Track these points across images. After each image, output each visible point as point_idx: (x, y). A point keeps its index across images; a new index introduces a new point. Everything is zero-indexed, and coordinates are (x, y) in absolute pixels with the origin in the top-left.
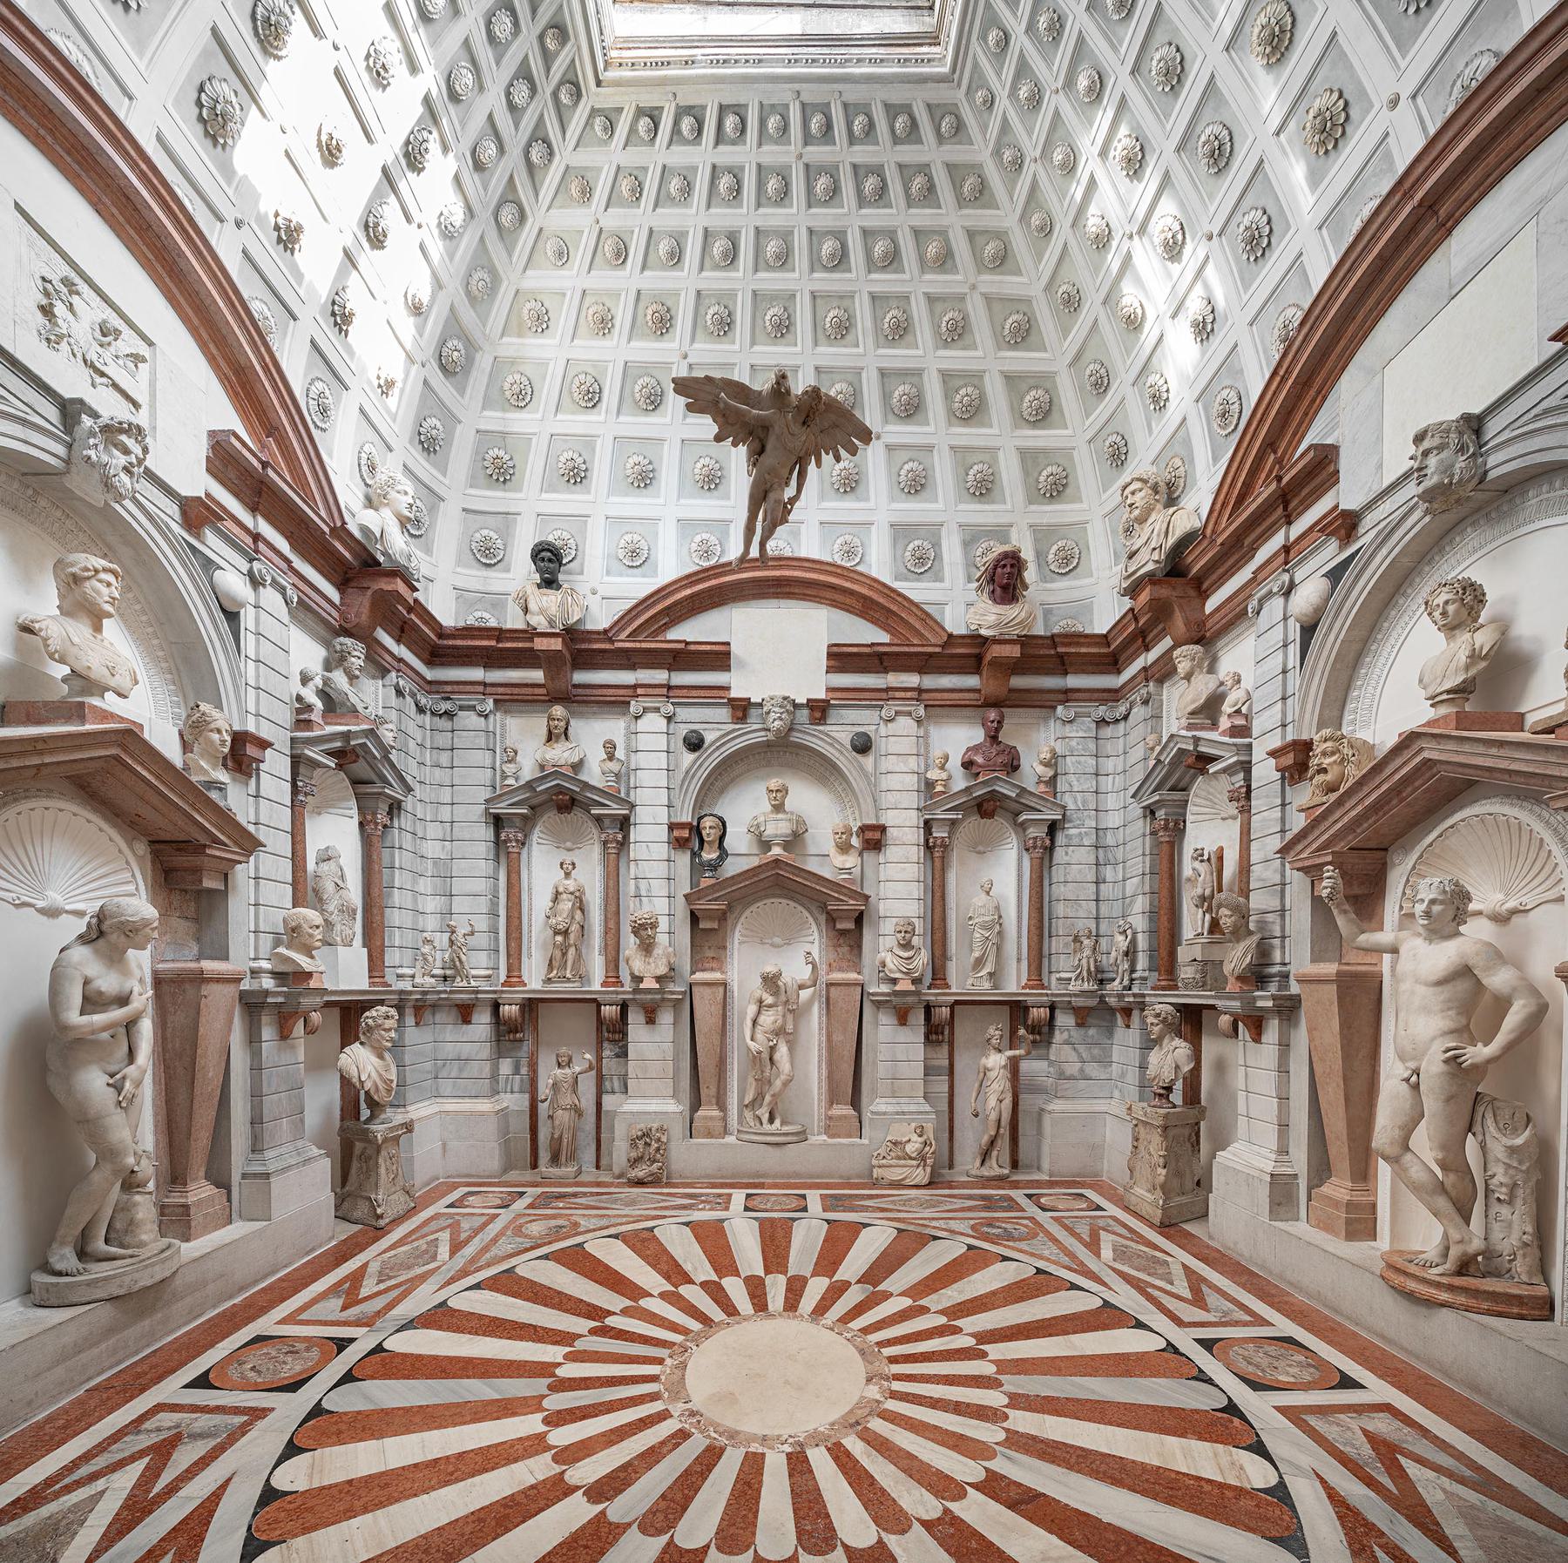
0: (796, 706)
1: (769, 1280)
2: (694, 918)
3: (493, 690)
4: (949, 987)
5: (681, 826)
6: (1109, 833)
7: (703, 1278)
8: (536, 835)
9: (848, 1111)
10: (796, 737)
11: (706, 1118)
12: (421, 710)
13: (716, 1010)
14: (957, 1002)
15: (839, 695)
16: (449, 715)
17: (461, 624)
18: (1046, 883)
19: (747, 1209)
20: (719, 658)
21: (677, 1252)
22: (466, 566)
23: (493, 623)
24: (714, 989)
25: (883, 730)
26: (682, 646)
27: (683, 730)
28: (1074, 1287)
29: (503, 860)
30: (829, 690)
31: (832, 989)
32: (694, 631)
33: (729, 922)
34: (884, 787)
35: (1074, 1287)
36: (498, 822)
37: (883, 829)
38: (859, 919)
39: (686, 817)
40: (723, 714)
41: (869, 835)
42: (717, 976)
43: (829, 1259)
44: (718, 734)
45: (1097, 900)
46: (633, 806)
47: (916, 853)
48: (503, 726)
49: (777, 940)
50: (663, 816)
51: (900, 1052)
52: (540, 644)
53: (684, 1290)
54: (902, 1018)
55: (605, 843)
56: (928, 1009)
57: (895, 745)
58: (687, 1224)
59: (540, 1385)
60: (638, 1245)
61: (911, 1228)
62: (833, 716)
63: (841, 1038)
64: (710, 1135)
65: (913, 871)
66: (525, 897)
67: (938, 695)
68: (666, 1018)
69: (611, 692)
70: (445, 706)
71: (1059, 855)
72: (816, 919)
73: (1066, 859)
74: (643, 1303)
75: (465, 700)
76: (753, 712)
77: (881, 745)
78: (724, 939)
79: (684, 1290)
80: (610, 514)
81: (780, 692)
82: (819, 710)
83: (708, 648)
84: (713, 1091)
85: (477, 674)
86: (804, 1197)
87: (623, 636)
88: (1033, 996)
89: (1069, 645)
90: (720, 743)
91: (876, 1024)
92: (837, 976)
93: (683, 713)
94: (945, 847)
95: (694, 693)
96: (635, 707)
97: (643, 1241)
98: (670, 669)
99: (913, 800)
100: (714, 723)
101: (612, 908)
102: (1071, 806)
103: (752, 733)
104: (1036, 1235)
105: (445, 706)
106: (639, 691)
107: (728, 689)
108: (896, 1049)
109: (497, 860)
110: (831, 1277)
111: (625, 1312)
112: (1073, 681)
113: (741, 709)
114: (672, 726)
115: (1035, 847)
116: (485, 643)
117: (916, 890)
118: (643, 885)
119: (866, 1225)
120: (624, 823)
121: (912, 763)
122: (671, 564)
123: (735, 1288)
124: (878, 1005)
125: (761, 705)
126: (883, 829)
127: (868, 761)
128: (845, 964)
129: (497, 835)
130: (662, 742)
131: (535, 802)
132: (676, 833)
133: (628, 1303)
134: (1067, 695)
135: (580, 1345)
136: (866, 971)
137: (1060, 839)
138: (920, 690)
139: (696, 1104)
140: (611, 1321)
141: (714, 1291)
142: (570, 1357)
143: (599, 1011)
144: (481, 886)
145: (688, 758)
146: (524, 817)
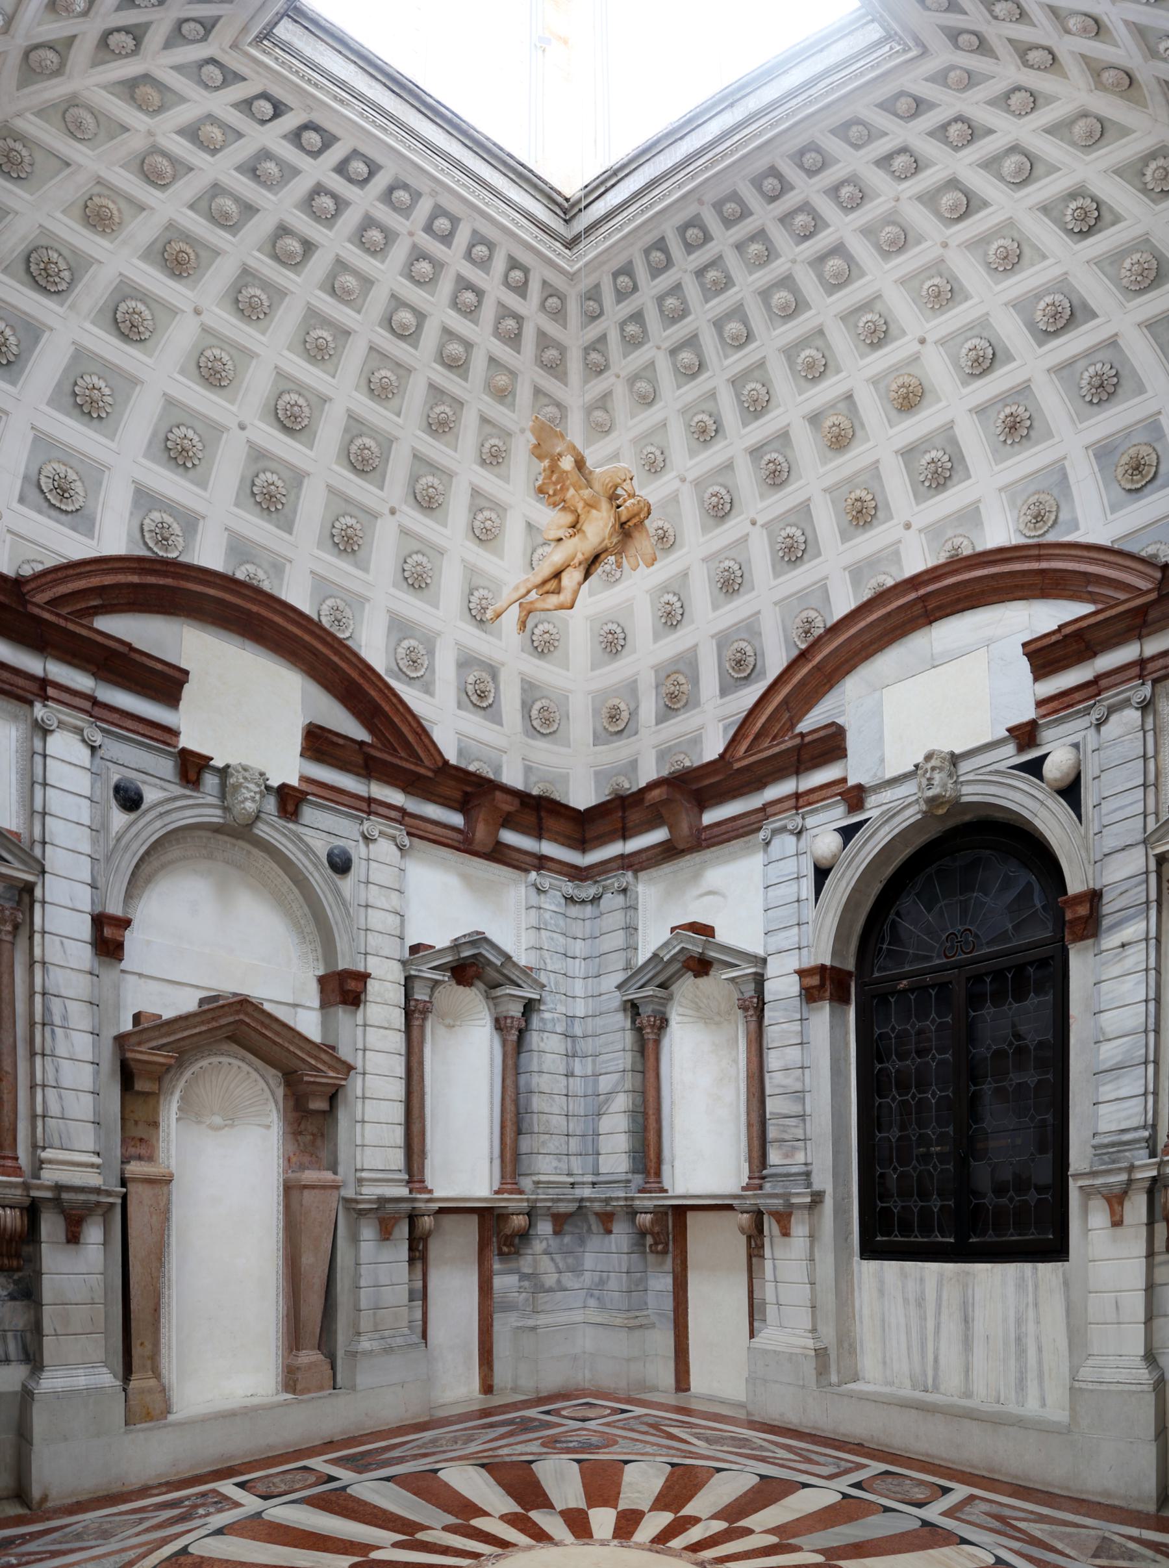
10: (262, 830)
20: (166, 683)
30: (304, 779)
37: (364, 977)
38: (333, 1098)
40: (166, 767)
47: (398, 1018)
49: (217, 1120)
56: (413, 1218)
62: (309, 814)
76: (210, 781)
77: (358, 869)
78: (156, 1111)
81: (256, 762)
82: (290, 801)
83: (159, 667)
93: (116, 749)
103: (203, 807)
107: (175, 733)
113: (192, 768)
114: (97, 760)
124: (361, 1213)
125: (224, 772)
126: (364, 977)
127: (347, 885)
128: (306, 1159)
130: (82, 783)
136: (341, 1169)
138: (402, 811)
145: (119, 818)
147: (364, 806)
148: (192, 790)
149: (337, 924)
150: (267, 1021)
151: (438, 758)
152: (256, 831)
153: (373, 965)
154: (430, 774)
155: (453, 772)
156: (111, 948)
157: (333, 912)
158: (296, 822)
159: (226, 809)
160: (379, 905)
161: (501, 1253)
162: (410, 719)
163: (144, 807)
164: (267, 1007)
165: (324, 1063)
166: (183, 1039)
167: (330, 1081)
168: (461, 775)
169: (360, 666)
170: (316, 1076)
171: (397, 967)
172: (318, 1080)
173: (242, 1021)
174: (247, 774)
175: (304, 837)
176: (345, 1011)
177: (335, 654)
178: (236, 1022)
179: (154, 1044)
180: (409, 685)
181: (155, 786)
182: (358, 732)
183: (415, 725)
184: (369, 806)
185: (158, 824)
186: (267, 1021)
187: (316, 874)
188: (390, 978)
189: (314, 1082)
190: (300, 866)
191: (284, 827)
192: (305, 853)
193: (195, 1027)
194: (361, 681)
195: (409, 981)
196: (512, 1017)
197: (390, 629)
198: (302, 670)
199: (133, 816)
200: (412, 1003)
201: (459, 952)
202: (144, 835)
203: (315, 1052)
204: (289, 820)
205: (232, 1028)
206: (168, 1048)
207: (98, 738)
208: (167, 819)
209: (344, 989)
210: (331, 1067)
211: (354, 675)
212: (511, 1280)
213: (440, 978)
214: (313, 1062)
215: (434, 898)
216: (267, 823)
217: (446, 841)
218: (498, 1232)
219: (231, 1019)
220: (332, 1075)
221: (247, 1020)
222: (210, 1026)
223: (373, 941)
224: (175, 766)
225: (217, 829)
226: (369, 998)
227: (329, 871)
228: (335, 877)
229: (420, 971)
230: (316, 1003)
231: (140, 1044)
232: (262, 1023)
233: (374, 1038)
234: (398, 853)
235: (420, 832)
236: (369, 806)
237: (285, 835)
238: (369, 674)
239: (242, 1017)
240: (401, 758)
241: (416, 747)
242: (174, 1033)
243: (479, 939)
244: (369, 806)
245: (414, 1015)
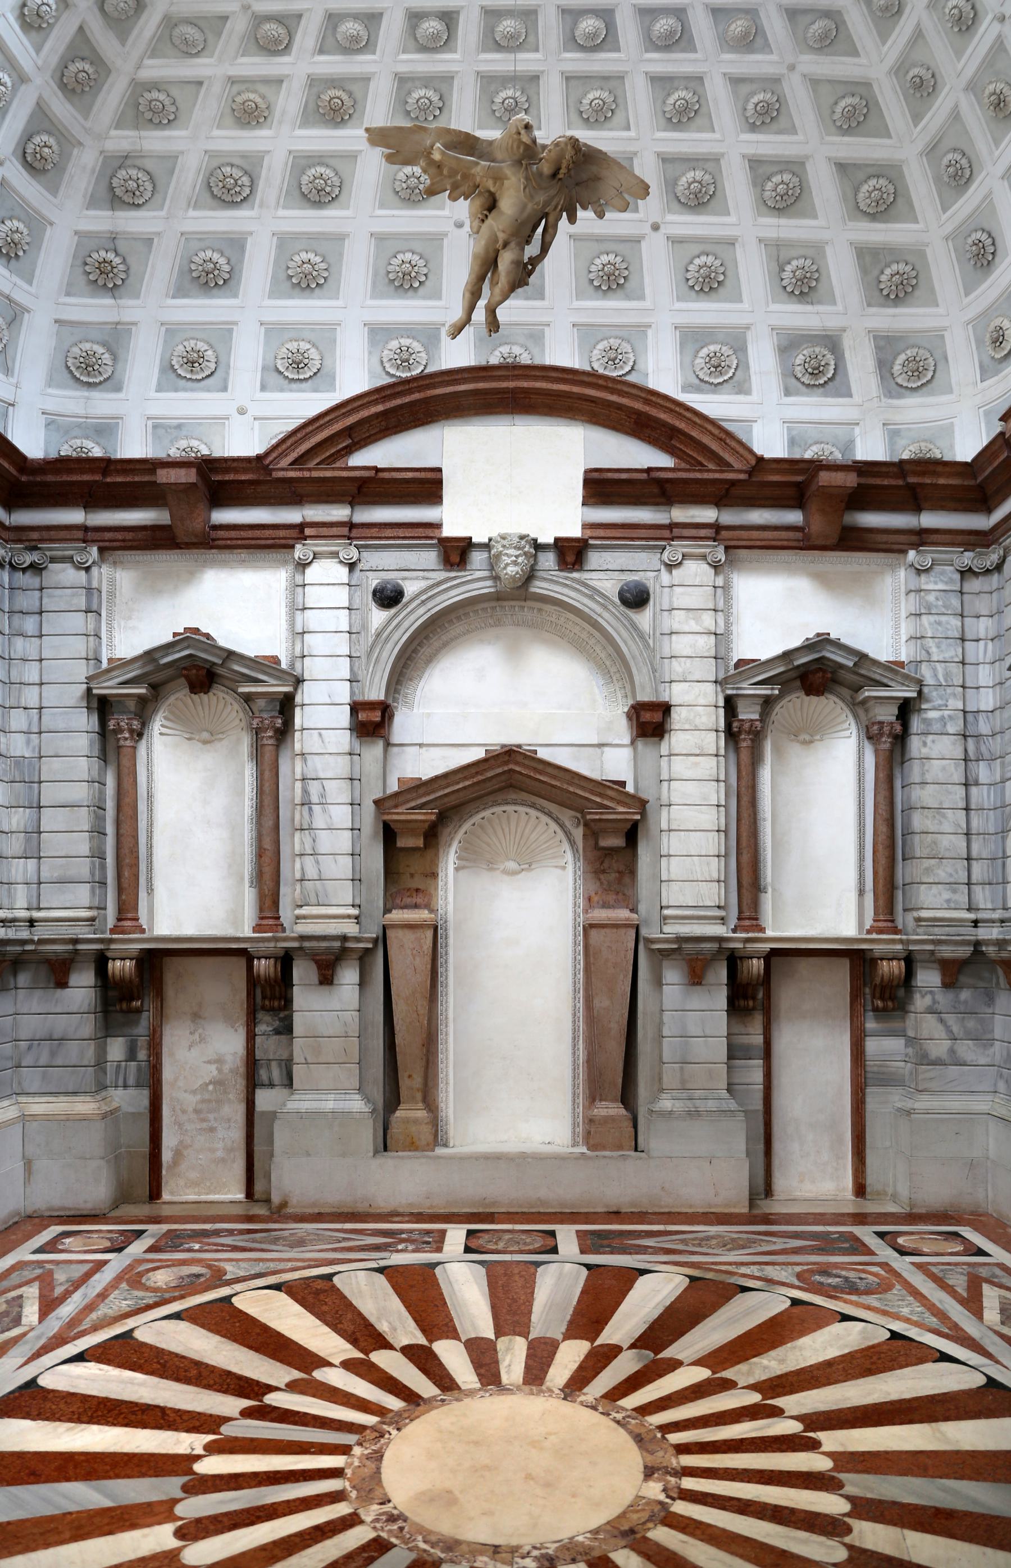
0: (538, 547)
1: (502, 1344)
2: (389, 834)
3: (97, 536)
4: (762, 930)
5: (371, 706)
6: (981, 717)
7: (405, 1341)
8: (157, 725)
9: (614, 1109)
11: (407, 1121)
13: (423, 963)
14: (774, 952)
15: (601, 533)
16: (35, 568)
17: (53, 455)
18: (898, 784)
21: (367, 1307)
22: (59, 386)
23: (97, 452)
24: (419, 933)
25: (665, 577)
28: (945, 1357)
29: (111, 756)
30: (586, 526)
31: (593, 933)
33: (443, 838)
34: (666, 653)
35: (945, 1357)
36: (102, 706)
39: (376, 693)
40: (430, 558)
41: (647, 716)
42: (423, 915)
43: (592, 1313)
44: (423, 584)
45: (967, 809)
46: (299, 681)
47: (713, 741)
48: (112, 582)
50: (343, 693)
51: (693, 1023)
52: (164, 476)
53: (380, 1358)
54: (696, 977)
55: (258, 732)
57: (683, 598)
58: (381, 1270)
59: (171, 1486)
60: (310, 1299)
61: (710, 1275)
62: (594, 559)
63: (606, 1003)
64: (412, 1146)
65: (709, 766)
66: (142, 807)
67: (744, 534)
68: (349, 976)
69: (267, 533)
70: (28, 558)
71: (915, 744)
72: (568, 834)
73: (925, 751)
74: (319, 1374)
75: (58, 549)
76: (478, 558)
77: (659, 599)
79: (380, 1358)
80: (265, 319)
84: (418, 1081)
85: (75, 516)
87: (284, 463)
88: (884, 944)
89: (923, 474)
90: (424, 596)
91: (658, 982)
92: (601, 915)
94: (757, 736)
95: (389, 532)
97: (317, 1293)
99: (708, 670)
100: (416, 571)
101: (269, 823)
102: (929, 680)
103: (474, 581)
104: (889, 1288)
105: (28, 558)
106: (308, 531)
107: (438, 526)
108: (690, 1019)
109: (104, 757)
110: (592, 1340)
111: (293, 1387)
112: (929, 520)
115: (881, 734)
116: (86, 478)
117: (714, 793)
118: (314, 788)
120: (286, 705)
121: (708, 620)
123: (451, 1354)
126: (666, 709)
127: (644, 618)
129: (103, 722)
131: (156, 678)
132: (362, 716)
133: (297, 1374)
134: (922, 538)
135: (227, 1430)
137: (916, 724)
139: (393, 1100)
140: (272, 1399)
141: (422, 1358)
142: (212, 1449)
144: (81, 793)
145: (378, 616)
146: (142, 700)
148: (460, 571)
149: (634, 658)
150: (540, 767)
151: (749, 457)
152: (533, 590)
153: (677, 694)
154: (742, 476)
155: (774, 466)
156: (371, 729)
157: (629, 647)
158: (581, 569)
159: (496, 578)
160: (687, 629)
161: (875, 1010)
162: (710, 427)
164: (543, 754)
165: (612, 799)
166: (446, 795)
167: (619, 817)
168: (786, 466)
169: (643, 395)
170: (601, 813)
171: (710, 688)
172: (604, 817)
173: (511, 770)
174: (505, 542)
175: (590, 582)
176: (646, 744)
177: (612, 393)
178: (504, 773)
179: (413, 804)
180: (714, 392)
181: (417, 578)
182: (661, 460)
183: (716, 432)
184: (672, 531)
185: (422, 610)
186: (540, 767)
187: (606, 615)
188: (702, 702)
189: (600, 820)
190: (586, 610)
191: (566, 578)
192: (591, 597)
193: (458, 783)
194: (646, 408)
195: (730, 705)
196: (881, 723)
197: (682, 345)
198: (583, 421)
199: (393, 611)
200: (735, 724)
201: (792, 661)
202: (406, 624)
203: (600, 790)
204: (573, 570)
205: (503, 778)
206: (432, 805)
208: (430, 605)
209: (651, 722)
210: (619, 802)
211: (638, 406)
212: (894, 1045)
213: (769, 692)
214: (598, 800)
215: (778, 609)
216: (545, 579)
217: (779, 543)
218: (874, 982)
219: (500, 770)
221: (518, 769)
222: (475, 780)
223: (678, 667)
224: (439, 556)
225: (498, 597)
226: (675, 726)
227: (622, 608)
228: (630, 613)
229: (738, 689)
231: (396, 806)
232: (535, 769)
233: (679, 766)
234: (713, 571)
236: (672, 531)
237: (566, 585)
238: (654, 399)
239: (512, 766)
240: (709, 471)
241: (721, 453)
242: (433, 792)
243: (823, 641)
244: (671, 532)
245: (743, 736)
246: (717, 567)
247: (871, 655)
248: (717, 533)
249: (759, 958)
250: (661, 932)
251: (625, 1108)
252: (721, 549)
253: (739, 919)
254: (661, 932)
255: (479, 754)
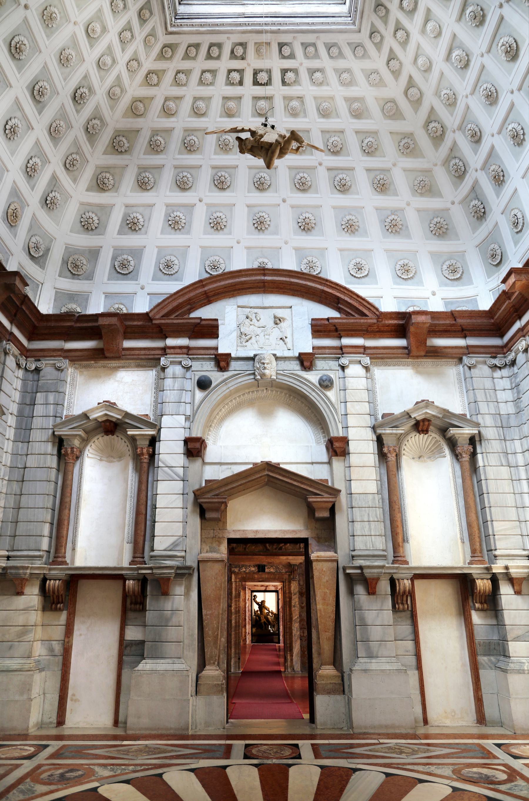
12: (18, 366)
19: (246, 757)
26: (199, 321)
27: (198, 375)
32: (205, 313)
37: (345, 441)
38: (332, 510)
86: (297, 746)
96: (163, 361)
98: (190, 338)
119: (355, 770)
122: (192, 274)
127: (331, 394)
138: (365, 348)
143: (125, 583)
145: (199, 395)
147: (339, 351)
163: (213, 385)
207: (187, 362)
209: (337, 448)
220: (327, 498)
230: (325, 459)
234: (364, 371)
235: (381, 357)
243: (427, 404)
246: (367, 369)
247: (451, 410)
248: (365, 351)
249: (408, 579)
250: (352, 564)
251: (337, 670)
252: (368, 358)
253: (394, 557)
254: (352, 564)
255: (251, 466)
